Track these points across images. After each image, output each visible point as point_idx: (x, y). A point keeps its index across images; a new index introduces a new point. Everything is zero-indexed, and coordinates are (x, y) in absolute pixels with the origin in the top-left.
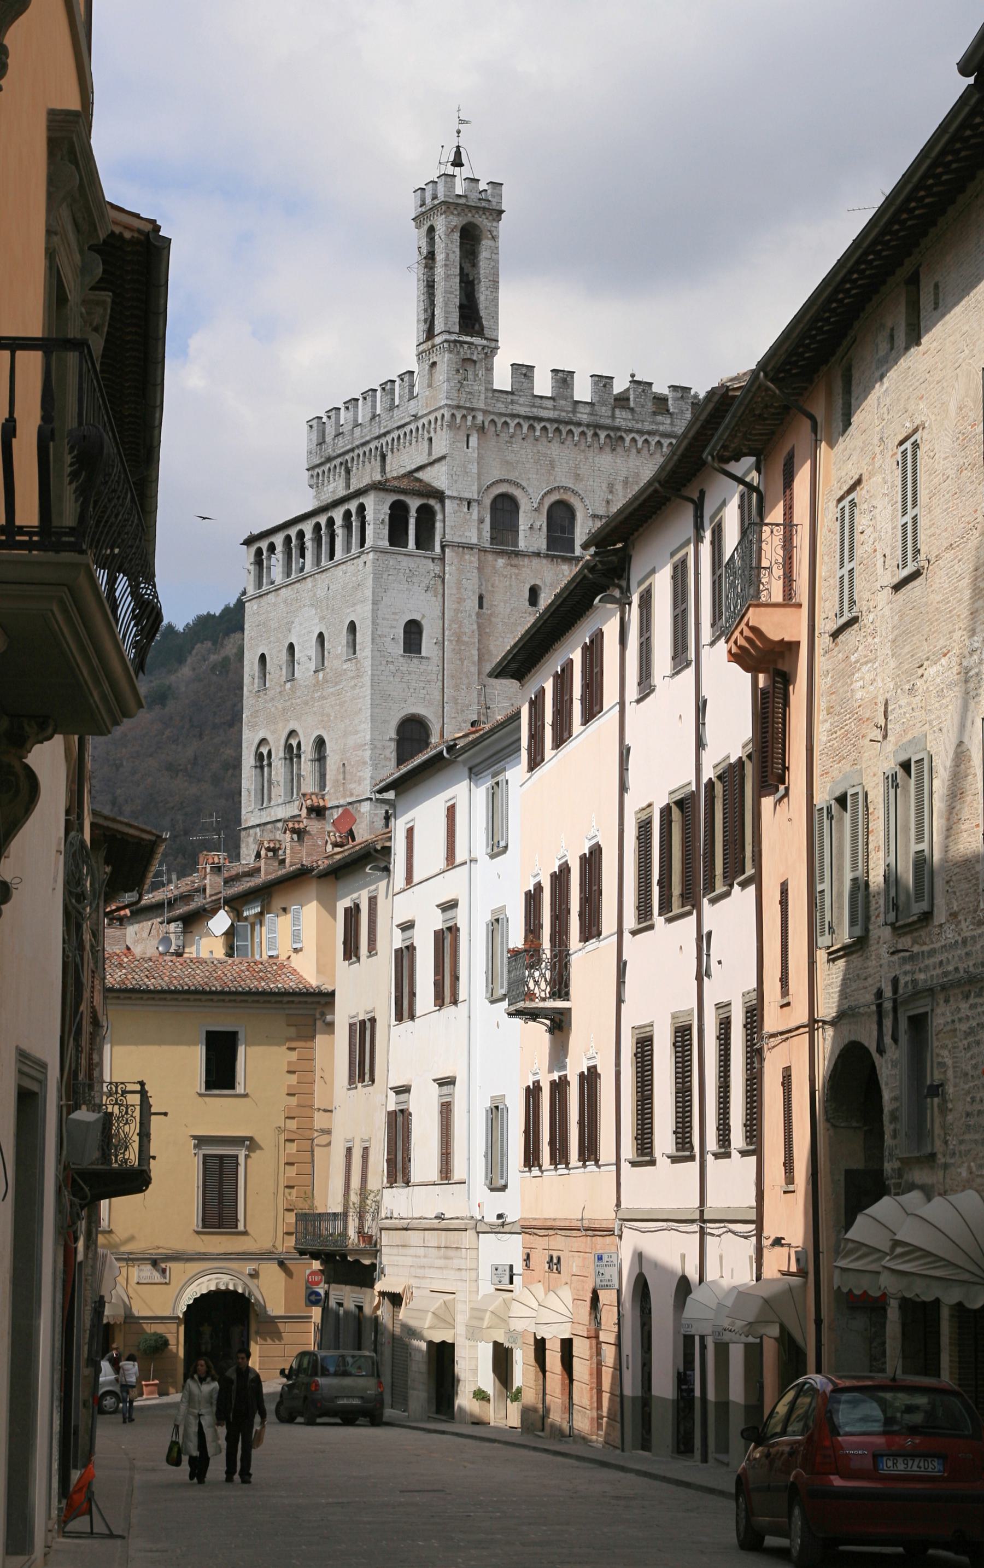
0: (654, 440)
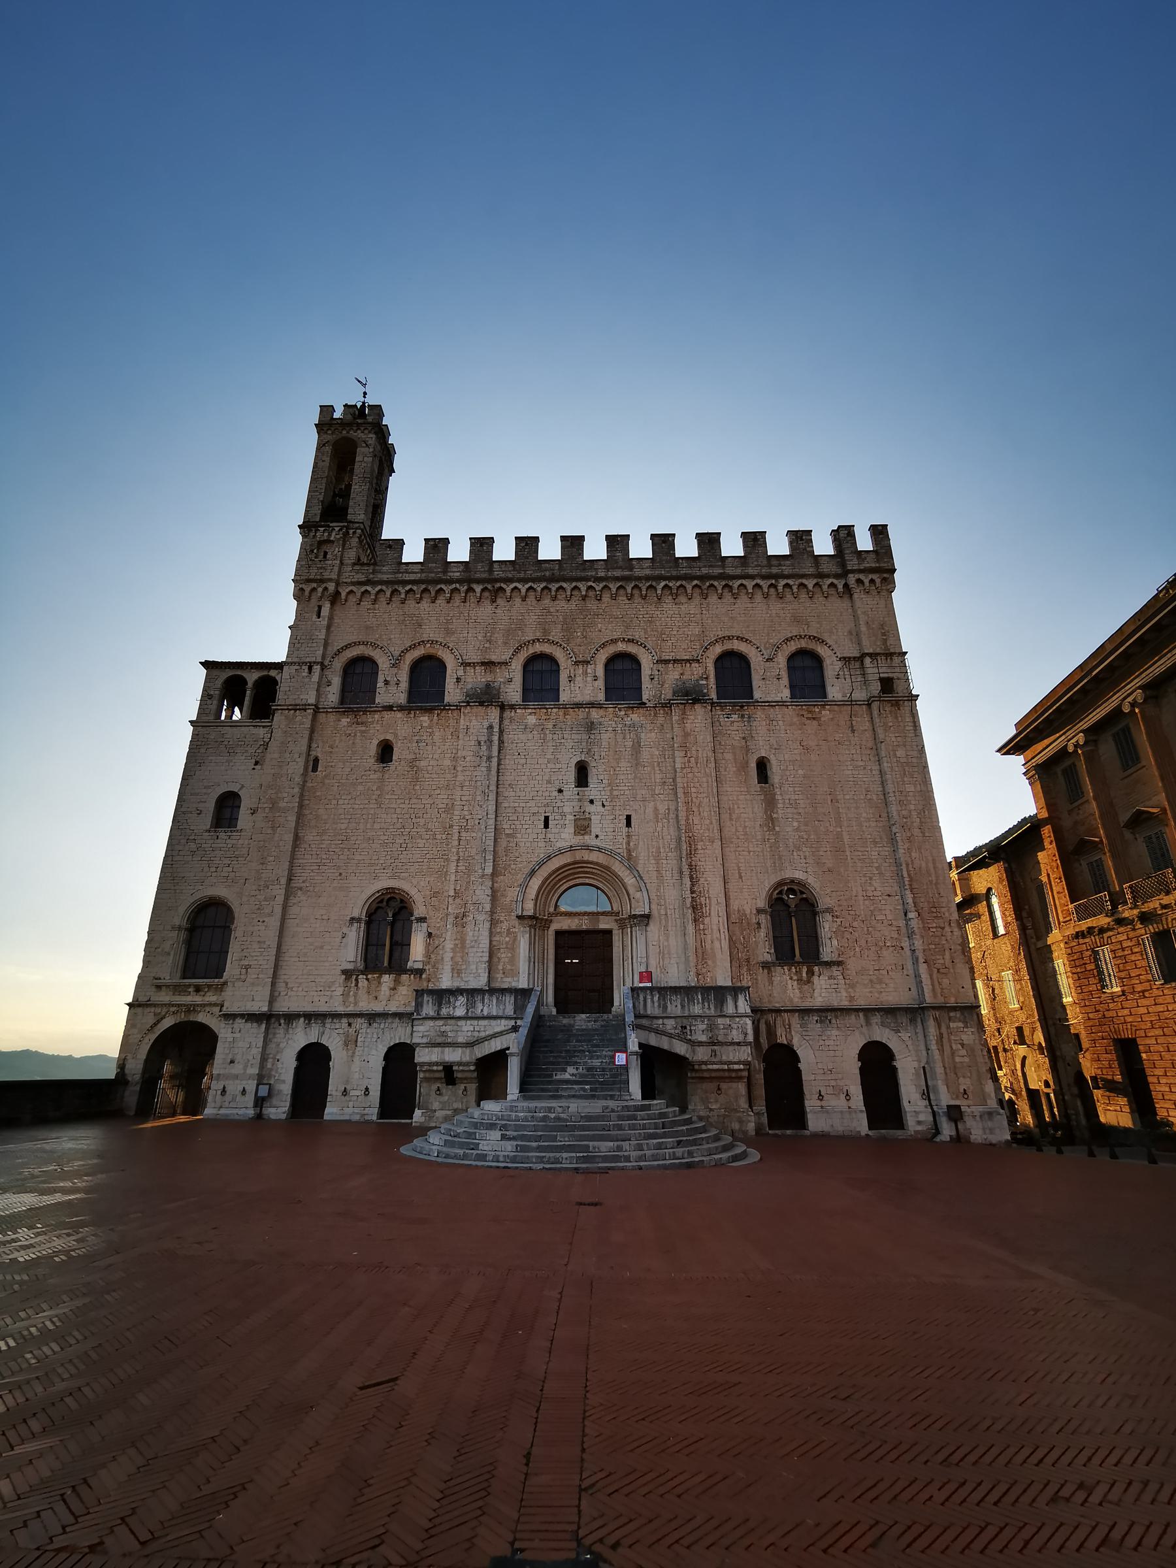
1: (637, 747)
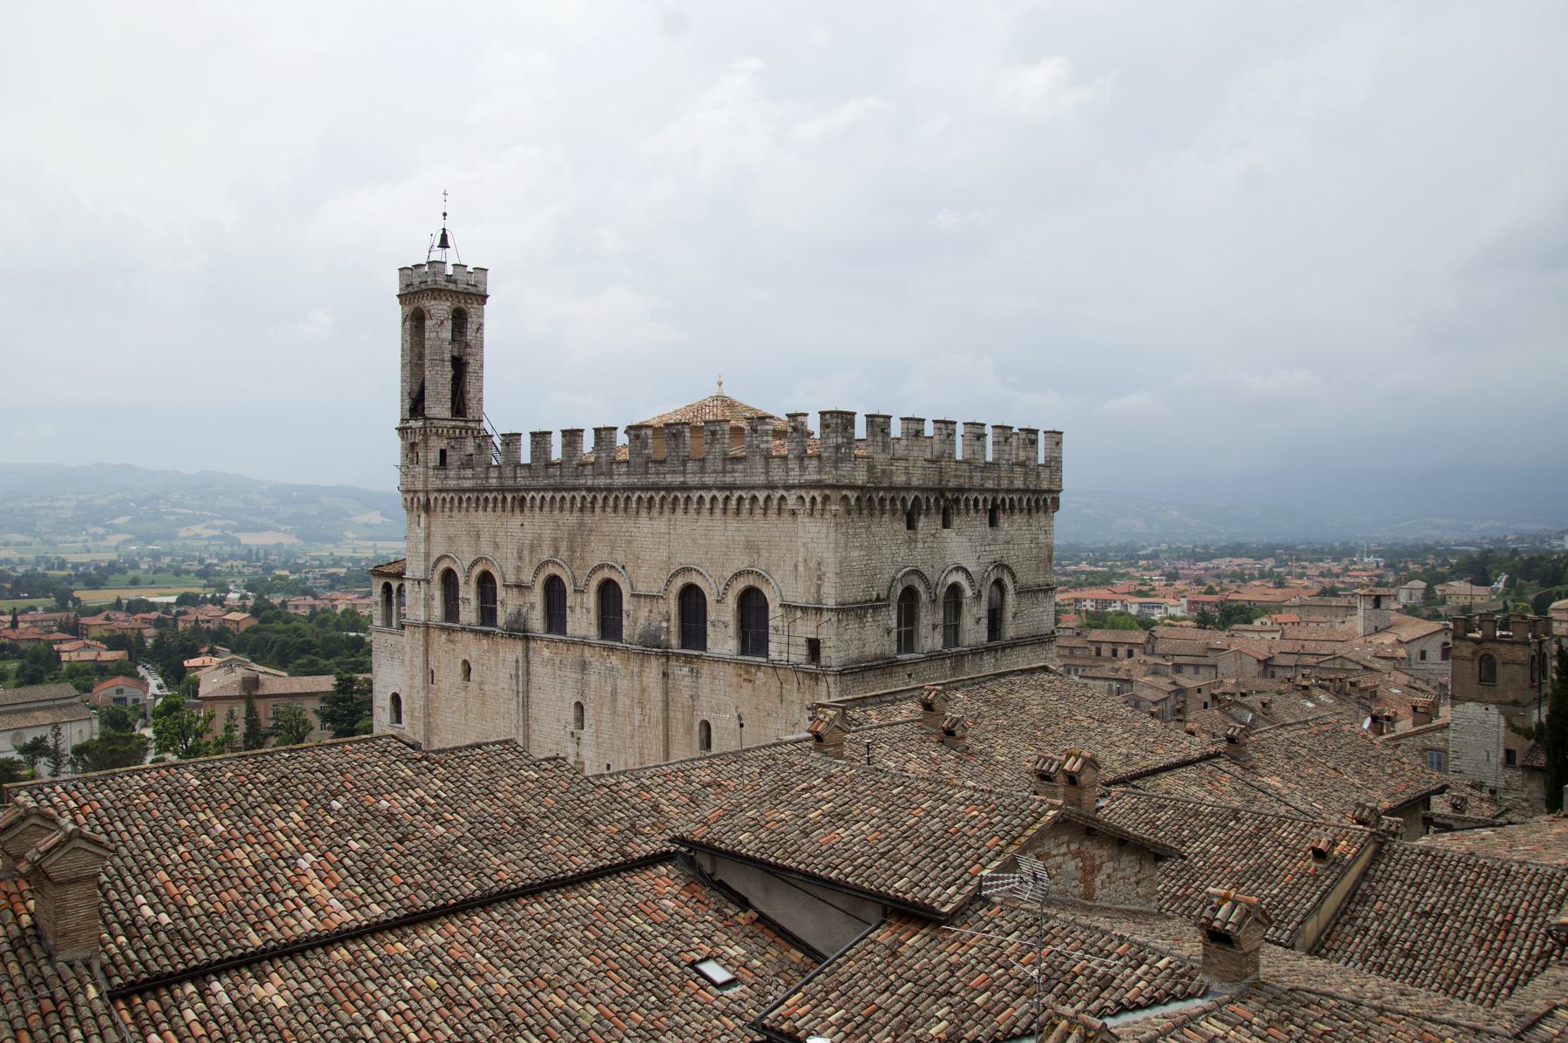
1: (614, 693)
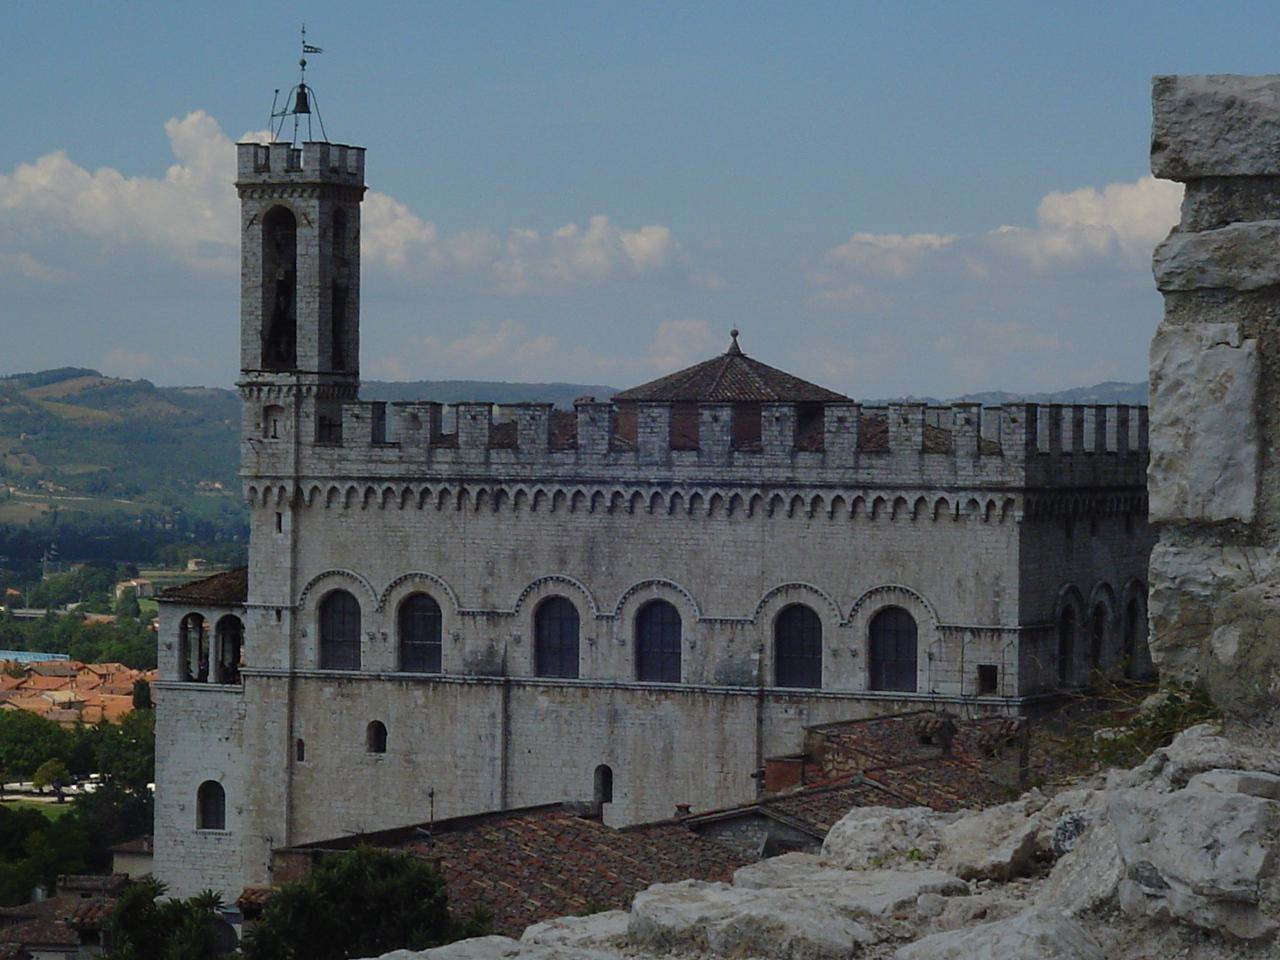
0: (551, 490)
1: (668, 751)
